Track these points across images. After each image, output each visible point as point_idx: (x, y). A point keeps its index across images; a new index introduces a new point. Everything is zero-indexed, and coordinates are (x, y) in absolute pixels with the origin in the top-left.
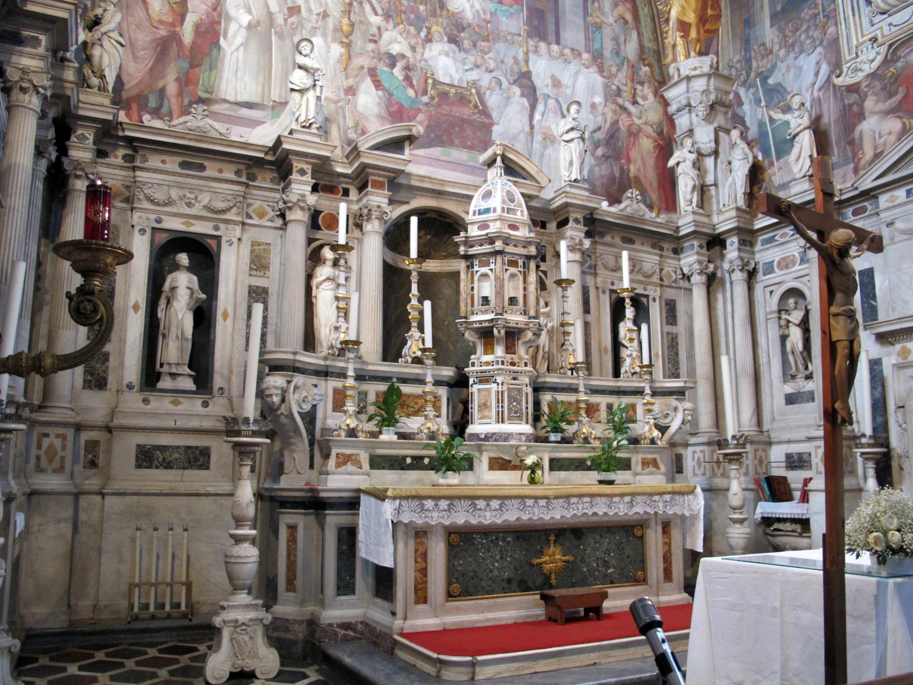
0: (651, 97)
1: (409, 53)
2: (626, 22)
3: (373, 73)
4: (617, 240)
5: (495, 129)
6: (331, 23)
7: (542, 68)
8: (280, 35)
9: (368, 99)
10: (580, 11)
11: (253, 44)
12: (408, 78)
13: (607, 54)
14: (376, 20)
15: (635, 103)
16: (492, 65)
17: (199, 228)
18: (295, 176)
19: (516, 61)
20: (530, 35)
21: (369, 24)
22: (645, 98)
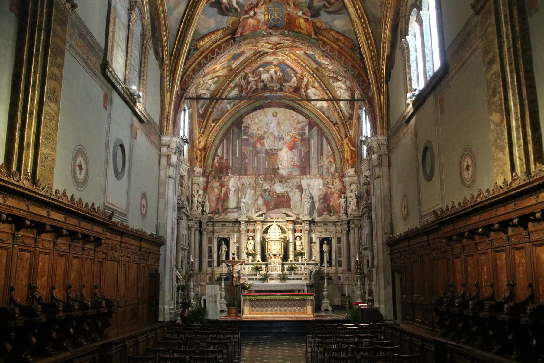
0: (338, 182)
1: (269, 188)
2: (331, 162)
3: (261, 195)
4: (322, 225)
5: (292, 201)
6: (251, 185)
7: (304, 183)
8: (241, 191)
9: (260, 201)
10: (317, 164)
11: (235, 195)
12: (269, 194)
13: (325, 173)
14: (261, 182)
15: (333, 185)
16: (291, 185)
17: (226, 236)
18: (242, 225)
19: (297, 183)
20: (301, 175)
21: (260, 183)
22: (336, 183)
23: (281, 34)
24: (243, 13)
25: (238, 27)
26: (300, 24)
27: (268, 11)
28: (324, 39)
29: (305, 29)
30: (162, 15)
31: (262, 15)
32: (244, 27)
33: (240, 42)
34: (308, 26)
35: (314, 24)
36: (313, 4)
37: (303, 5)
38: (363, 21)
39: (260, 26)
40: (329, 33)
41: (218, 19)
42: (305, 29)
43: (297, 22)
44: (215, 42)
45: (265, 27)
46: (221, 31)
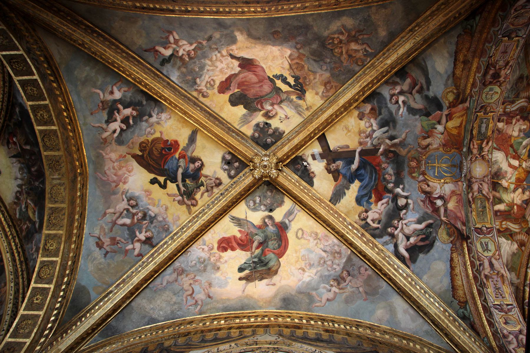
23: (466, 159)
24: (437, 217)
25: (456, 228)
26: (456, 128)
27: (440, 177)
28: (469, 85)
29: (461, 119)
30: (387, 337)
31: (442, 187)
32: (457, 218)
33: (470, 228)
34: (457, 115)
35: (452, 105)
36: (420, 110)
37: (425, 124)
38: (416, 29)
39: (458, 193)
40: (460, 79)
41: (436, 255)
42: (461, 119)
43: (455, 132)
44: (466, 270)
45: (460, 183)
46: (454, 255)
